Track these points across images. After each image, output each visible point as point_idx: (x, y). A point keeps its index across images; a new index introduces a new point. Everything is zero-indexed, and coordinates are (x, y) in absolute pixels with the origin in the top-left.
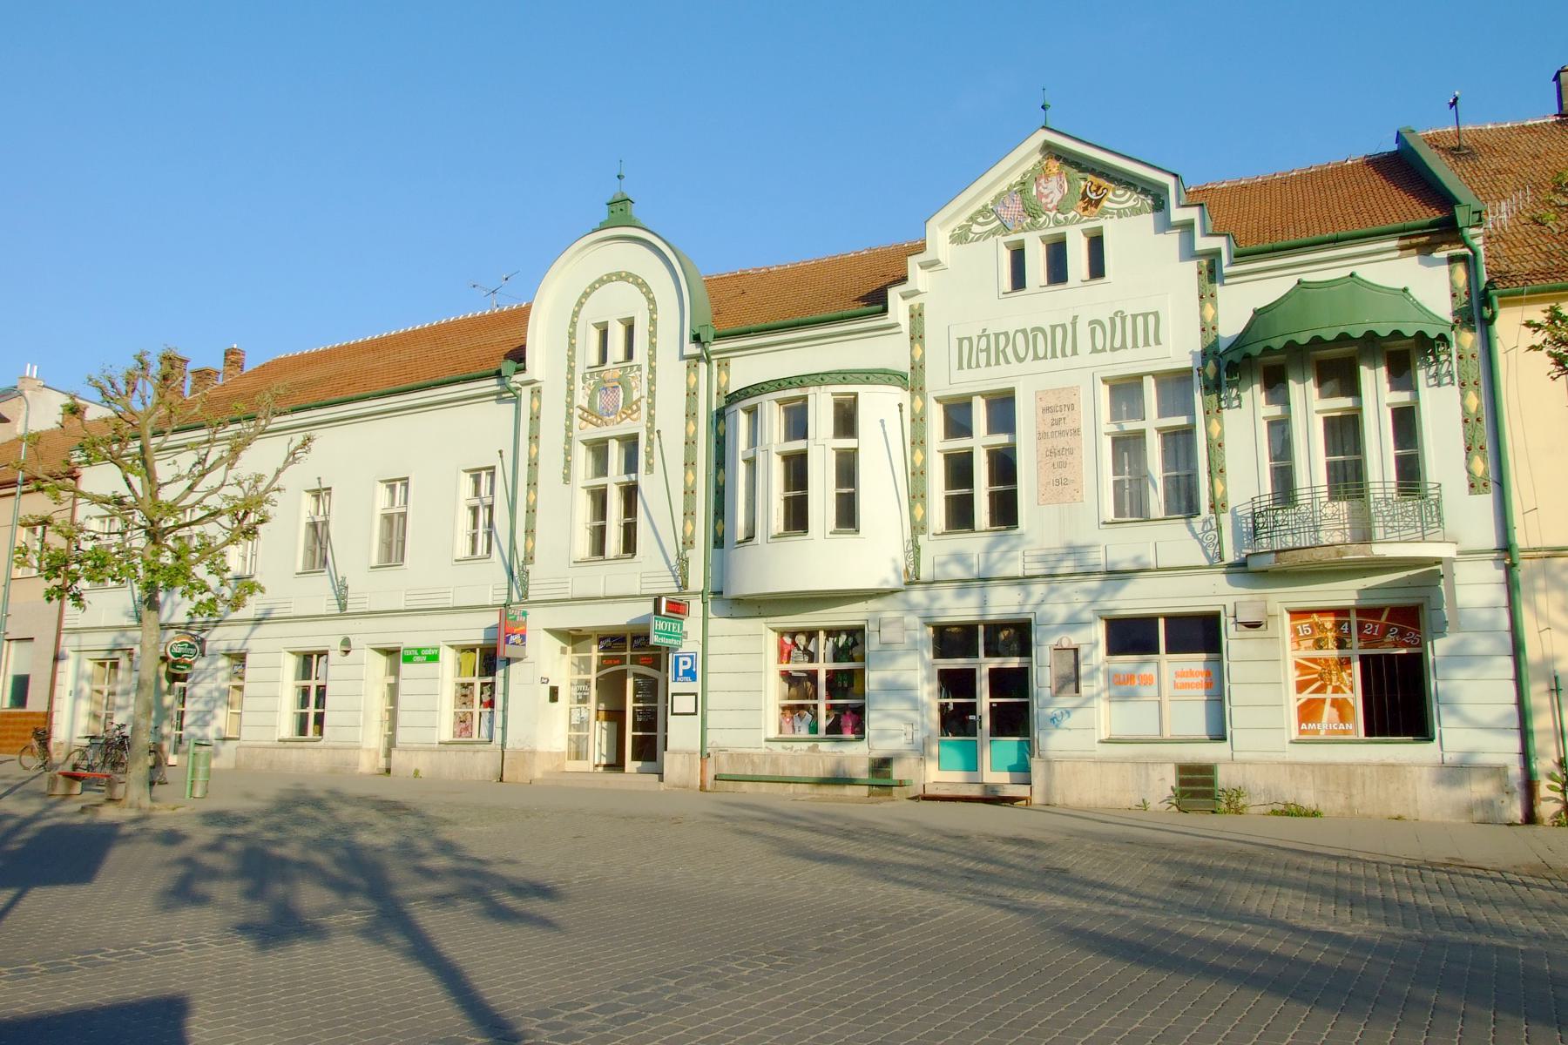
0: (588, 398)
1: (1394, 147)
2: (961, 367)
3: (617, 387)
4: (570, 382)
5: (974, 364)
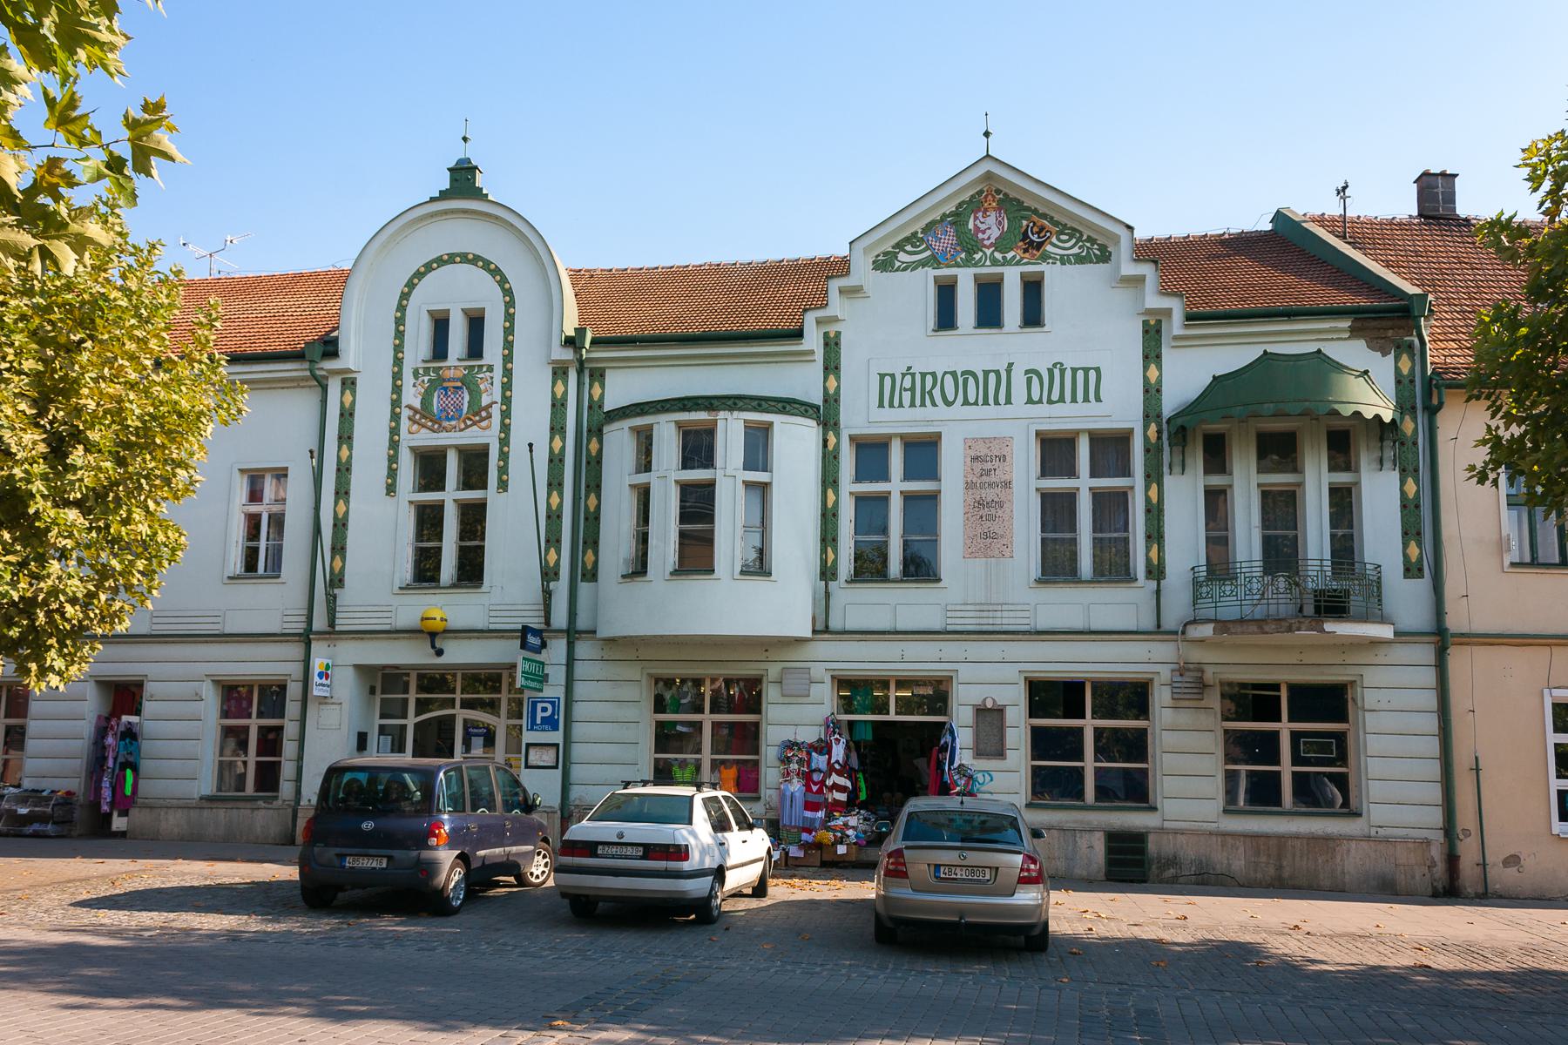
2: (881, 405)
3: (460, 388)
4: (397, 376)
5: (896, 403)
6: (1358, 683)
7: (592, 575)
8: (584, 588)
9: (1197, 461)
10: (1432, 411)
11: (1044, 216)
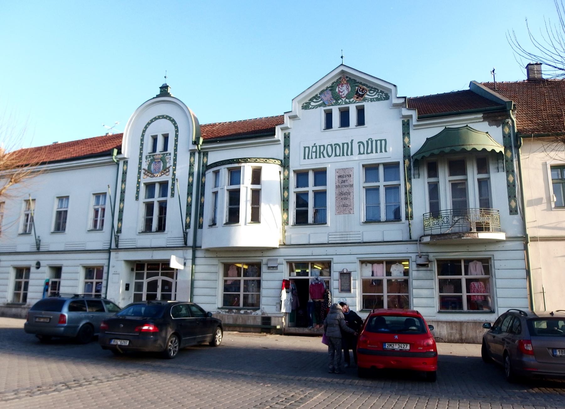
0: (147, 166)
1: (468, 88)
2: (305, 158)
3: (159, 162)
4: (141, 159)
5: (310, 157)
6: (492, 258)
7: (201, 226)
8: (199, 231)
9: (424, 173)
10: (518, 147)
11: (364, 85)
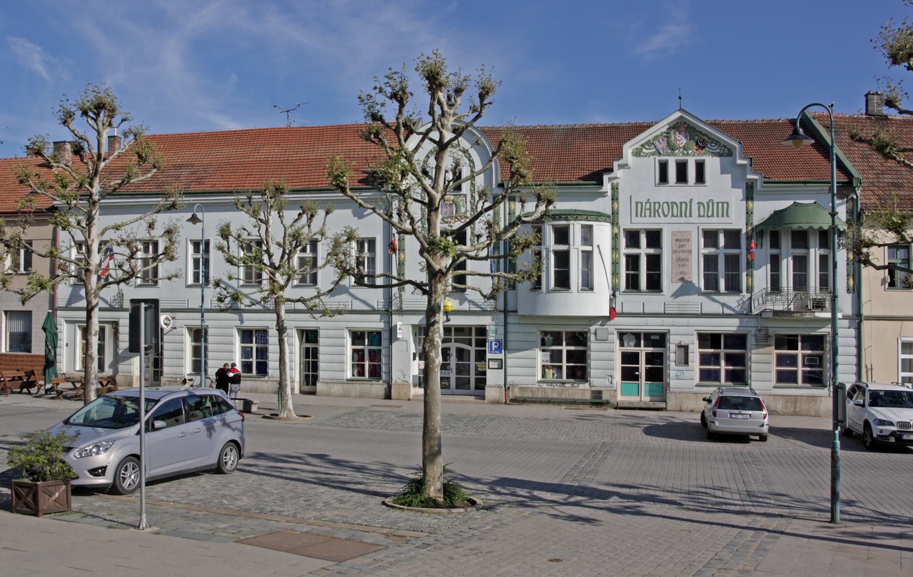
2: (637, 216)
5: (643, 215)
9: (767, 241)
11: (705, 135)
